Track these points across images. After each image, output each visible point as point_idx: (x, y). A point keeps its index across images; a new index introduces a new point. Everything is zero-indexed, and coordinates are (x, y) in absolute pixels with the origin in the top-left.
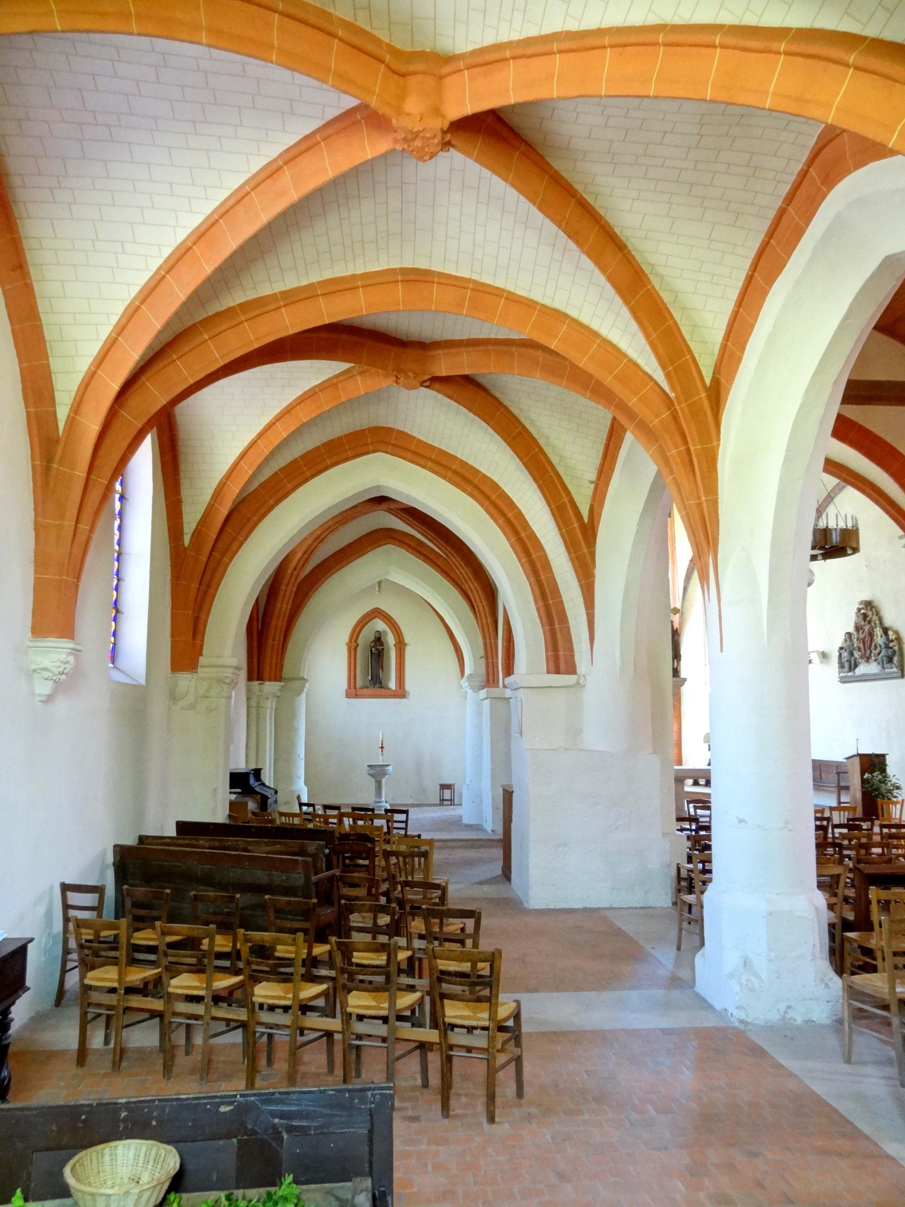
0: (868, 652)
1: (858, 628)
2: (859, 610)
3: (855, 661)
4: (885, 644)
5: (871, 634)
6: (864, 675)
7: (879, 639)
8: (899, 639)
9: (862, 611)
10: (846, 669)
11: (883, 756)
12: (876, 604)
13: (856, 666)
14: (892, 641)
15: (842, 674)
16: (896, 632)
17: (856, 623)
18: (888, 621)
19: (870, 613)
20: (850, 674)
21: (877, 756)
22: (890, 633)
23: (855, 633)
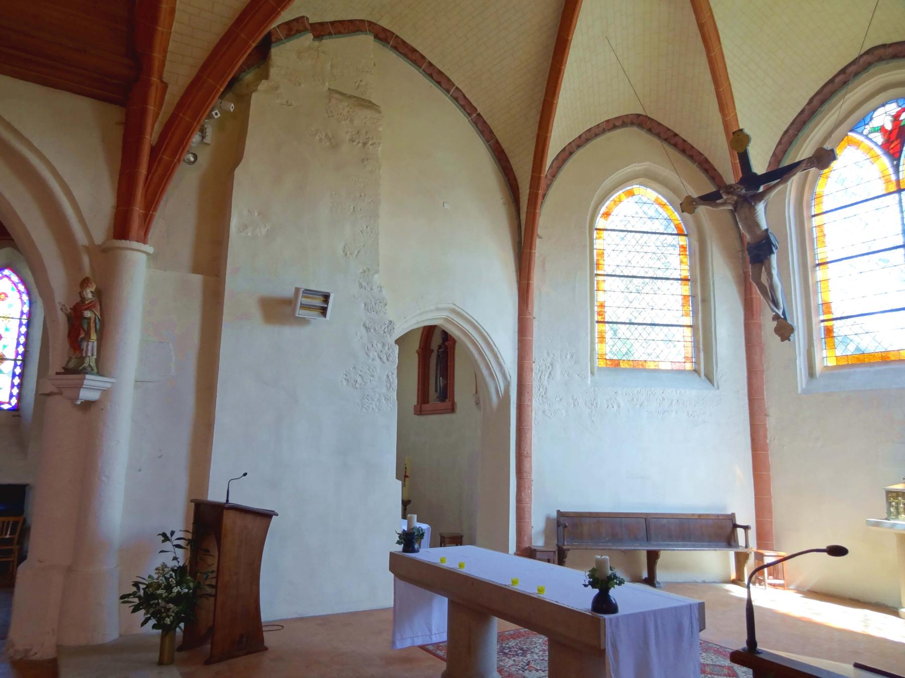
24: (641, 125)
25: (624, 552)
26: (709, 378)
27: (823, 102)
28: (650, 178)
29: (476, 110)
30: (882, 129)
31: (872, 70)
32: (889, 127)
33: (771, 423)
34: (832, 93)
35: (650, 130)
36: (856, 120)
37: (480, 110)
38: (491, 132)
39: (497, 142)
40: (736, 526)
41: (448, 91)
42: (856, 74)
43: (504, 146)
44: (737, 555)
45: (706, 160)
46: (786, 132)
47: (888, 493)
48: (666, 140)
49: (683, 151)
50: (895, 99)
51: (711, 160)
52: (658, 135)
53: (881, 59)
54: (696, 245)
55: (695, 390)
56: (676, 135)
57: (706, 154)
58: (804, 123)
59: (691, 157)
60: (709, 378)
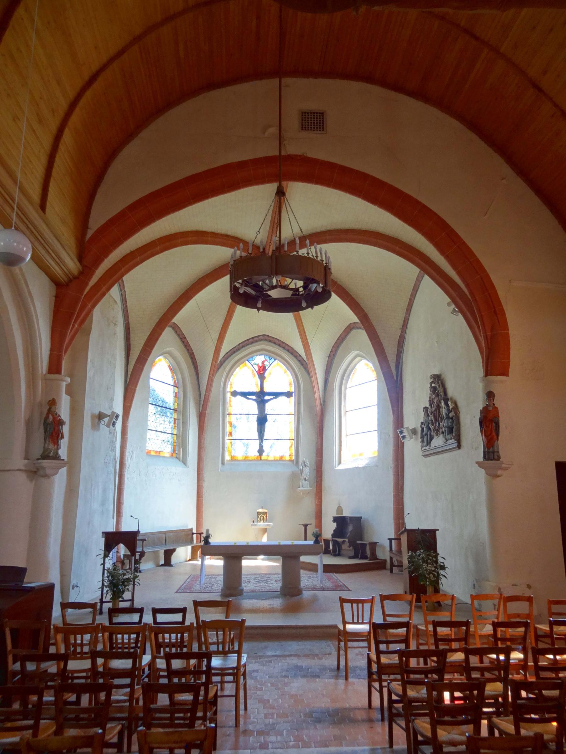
0: (437, 424)
1: (431, 402)
2: (431, 383)
3: (431, 435)
4: (446, 414)
5: (439, 407)
6: (436, 447)
7: (444, 411)
8: (456, 408)
9: (433, 385)
10: (425, 444)
11: (432, 533)
12: (443, 376)
13: (432, 439)
14: (451, 411)
15: (423, 448)
16: (455, 404)
17: (430, 398)
18: (451, 393)
19: (438, 387)
20: (428, 447)
21: (424, 532)
22: (450, 403)
23: (430, 407)
24: (174, 328)
25: (153, 552)
26: (184, 462)
27: (243, 347)
28: (169, 355)
29: (127, 303)
30: (258, 365)
31: (262, 342)
32: (261, 365)
33: (205, 485)
34: (247, 345)
35: (176, 332)
36: (249, 357)
37: (128, 305)
38: (128, 317)
39: (128, 323)
40: (193, 534)
41: (121, 291)
42: (257, 341)
43: (131, 326)
44: (193, 547)
45: (193, 353)
46: (227, 353)
47: (258, 513)
48: (181, 339)
49: (186, 346)
50: (265, 355)
51: (195, 354)
52: (179, 335)
53: (266, 340)
54: (181, 393)
55: (177, 468)
56: (185, 338)
57: (194, 351)
58: (234, 352)
59: (188, 350)
60: (184, 462)
